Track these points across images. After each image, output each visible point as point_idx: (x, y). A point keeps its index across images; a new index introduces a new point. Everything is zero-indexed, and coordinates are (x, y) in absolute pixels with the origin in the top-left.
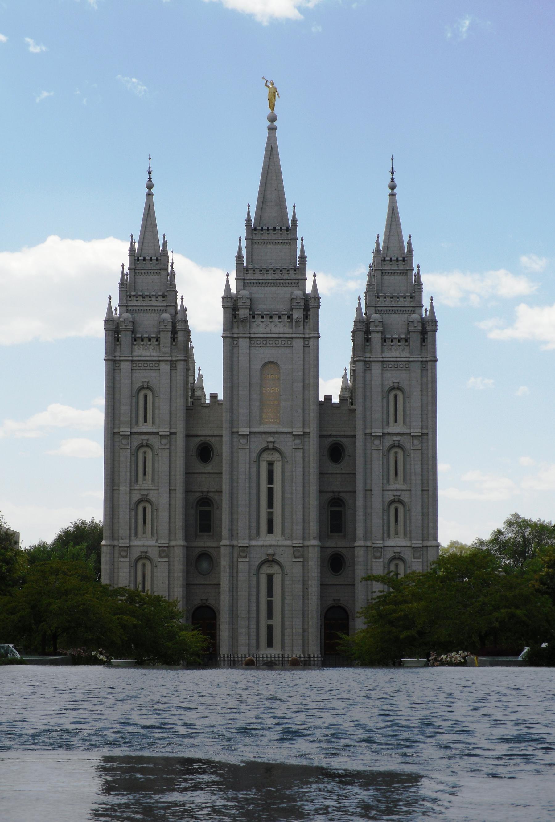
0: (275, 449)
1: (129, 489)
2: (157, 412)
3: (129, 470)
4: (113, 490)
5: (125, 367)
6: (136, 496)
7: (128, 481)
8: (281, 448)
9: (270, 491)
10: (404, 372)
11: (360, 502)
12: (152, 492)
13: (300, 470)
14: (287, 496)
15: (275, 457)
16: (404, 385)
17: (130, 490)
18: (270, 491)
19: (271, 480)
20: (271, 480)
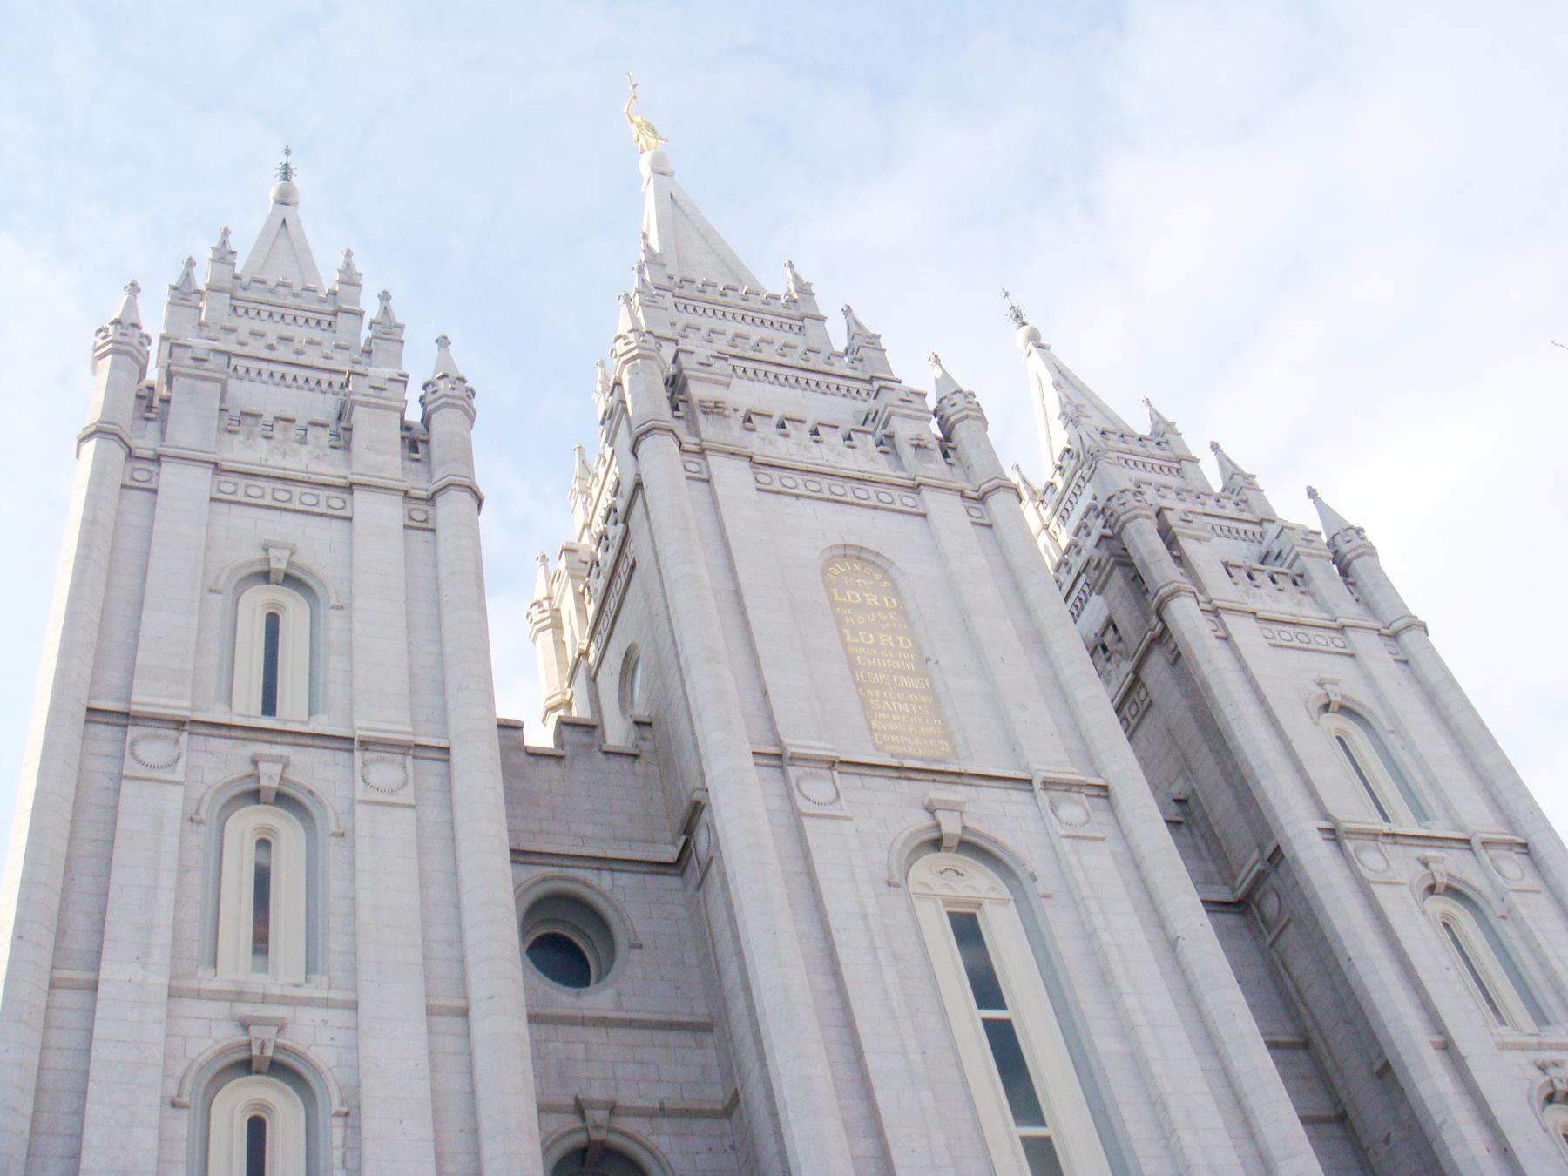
0: (971, 847)
1: (159, 981)
2: (335, 664)
3: (167, 880)
4: (53, 985)
5: (183, 486)
6: (210, 1033)
7: (163, 937)
8: (1005, 838)
9: (1003, 1041)
10: (1338, 659)
11: (1432, 1084)
12: (307, 1015)
13: (1124, 930)
14: (1105, 1043)
15: (976, 884)
16: (1359, 694)
17: (174, 994)
18: (1003, 1041)
19: (987, 990)
20: (987, 990)
